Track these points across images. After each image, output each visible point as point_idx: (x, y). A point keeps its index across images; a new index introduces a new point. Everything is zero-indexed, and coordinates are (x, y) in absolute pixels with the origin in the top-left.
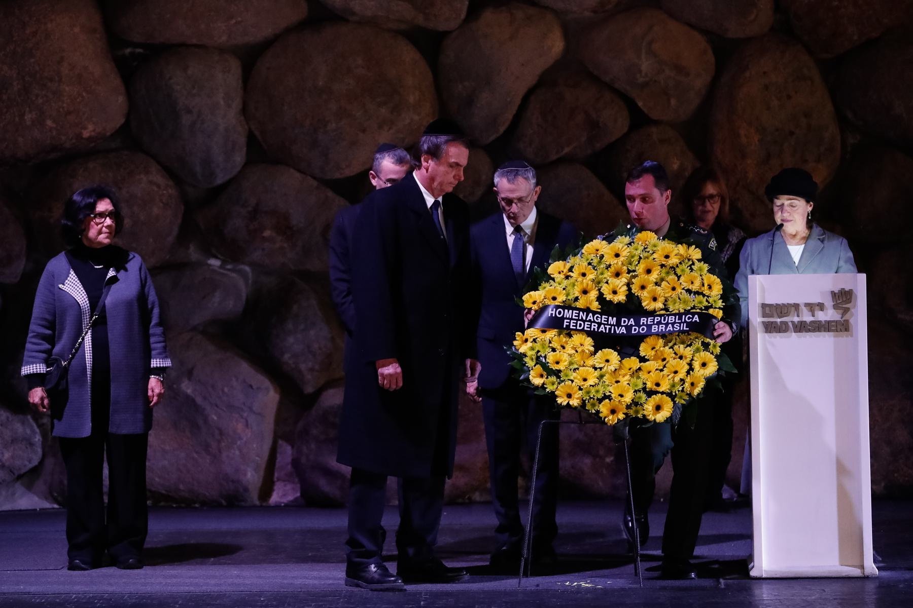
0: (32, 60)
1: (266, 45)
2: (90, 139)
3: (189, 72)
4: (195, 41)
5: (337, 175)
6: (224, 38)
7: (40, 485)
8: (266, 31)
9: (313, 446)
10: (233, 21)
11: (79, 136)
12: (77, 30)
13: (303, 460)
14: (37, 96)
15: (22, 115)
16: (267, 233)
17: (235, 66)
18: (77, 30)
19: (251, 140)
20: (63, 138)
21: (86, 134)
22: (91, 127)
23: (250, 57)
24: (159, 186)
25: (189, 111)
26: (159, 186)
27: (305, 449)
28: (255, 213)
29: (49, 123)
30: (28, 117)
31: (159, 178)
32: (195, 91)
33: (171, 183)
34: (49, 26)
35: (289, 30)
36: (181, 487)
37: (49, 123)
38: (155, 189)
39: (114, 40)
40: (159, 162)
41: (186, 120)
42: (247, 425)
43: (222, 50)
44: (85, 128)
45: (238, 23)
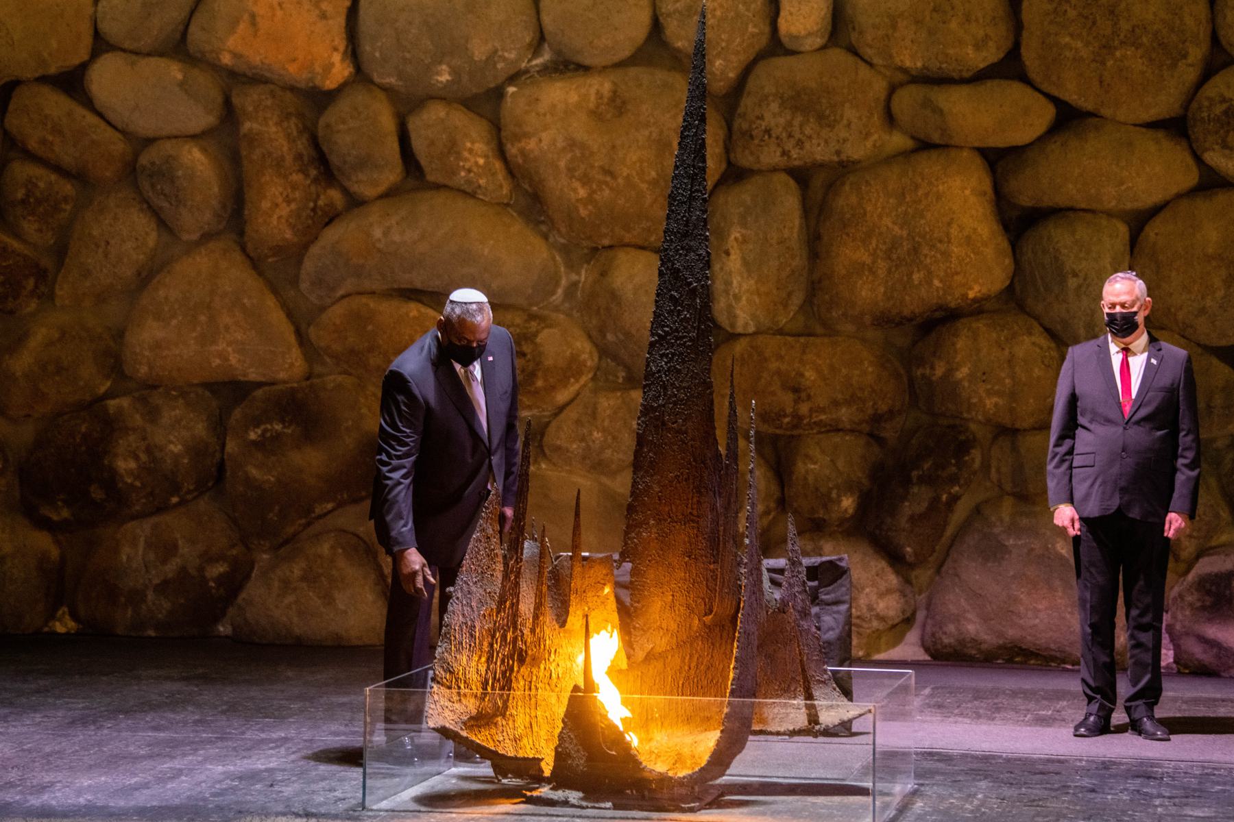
0: (923, 222)
1: (1155, 211)
2: (975, 300)
3: (1077, 237)
4: (1083, 206)
5: (1223, 343)
6: (1113, 203)
7: (913, 636)
8: (1156, 198)
9: (1187, 613)
10: (1123, 188)
11: (965, 296)
12: (967, 192)
13: (1178, 627)
14: (926, 256)
15: (910, 275)
17: (1123, 229)
18: (967, 192)
20: (949, 298)
21: (971, 295)
22: (977, 288)
23: (1139, 221)
24: (1041, 348)
25: (1075, 275)
26: (1041, 348)
27: (1180, 617)
29: (936, 283)
30: (916, 277)
31: (1044, 341)
32: (1082, 255)
33: (1053, 345)
34: (941, 188)
35: (1179, 196)
36: (1052, 646)
37: (936, 283)
38: (1038, 350)
39: (1001, 201)
40: (1041, 325)
41: (1072, 283)
43: (1110, 214)
44: (971, 288)
45: (1128, 188)
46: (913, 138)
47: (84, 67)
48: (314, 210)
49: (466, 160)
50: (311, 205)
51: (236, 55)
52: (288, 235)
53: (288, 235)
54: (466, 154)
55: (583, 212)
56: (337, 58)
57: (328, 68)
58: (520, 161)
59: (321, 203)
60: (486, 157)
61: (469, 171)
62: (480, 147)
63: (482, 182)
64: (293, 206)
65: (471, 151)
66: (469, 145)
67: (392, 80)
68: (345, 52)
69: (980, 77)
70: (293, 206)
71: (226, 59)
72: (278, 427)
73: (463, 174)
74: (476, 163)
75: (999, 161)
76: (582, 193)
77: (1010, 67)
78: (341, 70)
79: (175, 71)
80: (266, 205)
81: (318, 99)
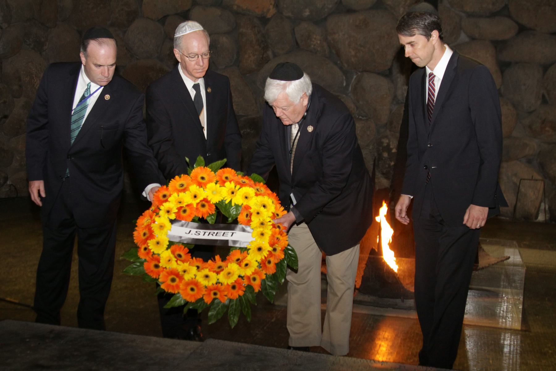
16: (547, 129)
19: (543, 96)
25: (524, 85)
28: (543, 122)
42: (534, 194)
46: (468, 36)
47: (189, 10)
48: (262, 58)
49: (313, 42)
50: (261, 56)
51: (238, 6)
52: (254, 66)
53: (254, 66)
54: (313, 40)
55: (353, 60)
56: (271, 7)
57: (269, 10)
58: (332, 42)
59: (264, 56)
60: (320, 41)
61: (315, 45)
62: (318, 37)
63: (319, 49)
64: (256, 57)
65: (315, 39)
66: (315, 36)
67: (290, 14)
68: (274, 5)
69: (493, 15)
70: (256, 57)
71: (235, 8)
72: (249, 131)
73: (312, 46)
74: (317, 43)
75: (499, 45)
76: (353, 53)
77: (503, 12)
78: (273, 11)
79: (218, 12)
80: (246, 56)
81: (264, 20)
